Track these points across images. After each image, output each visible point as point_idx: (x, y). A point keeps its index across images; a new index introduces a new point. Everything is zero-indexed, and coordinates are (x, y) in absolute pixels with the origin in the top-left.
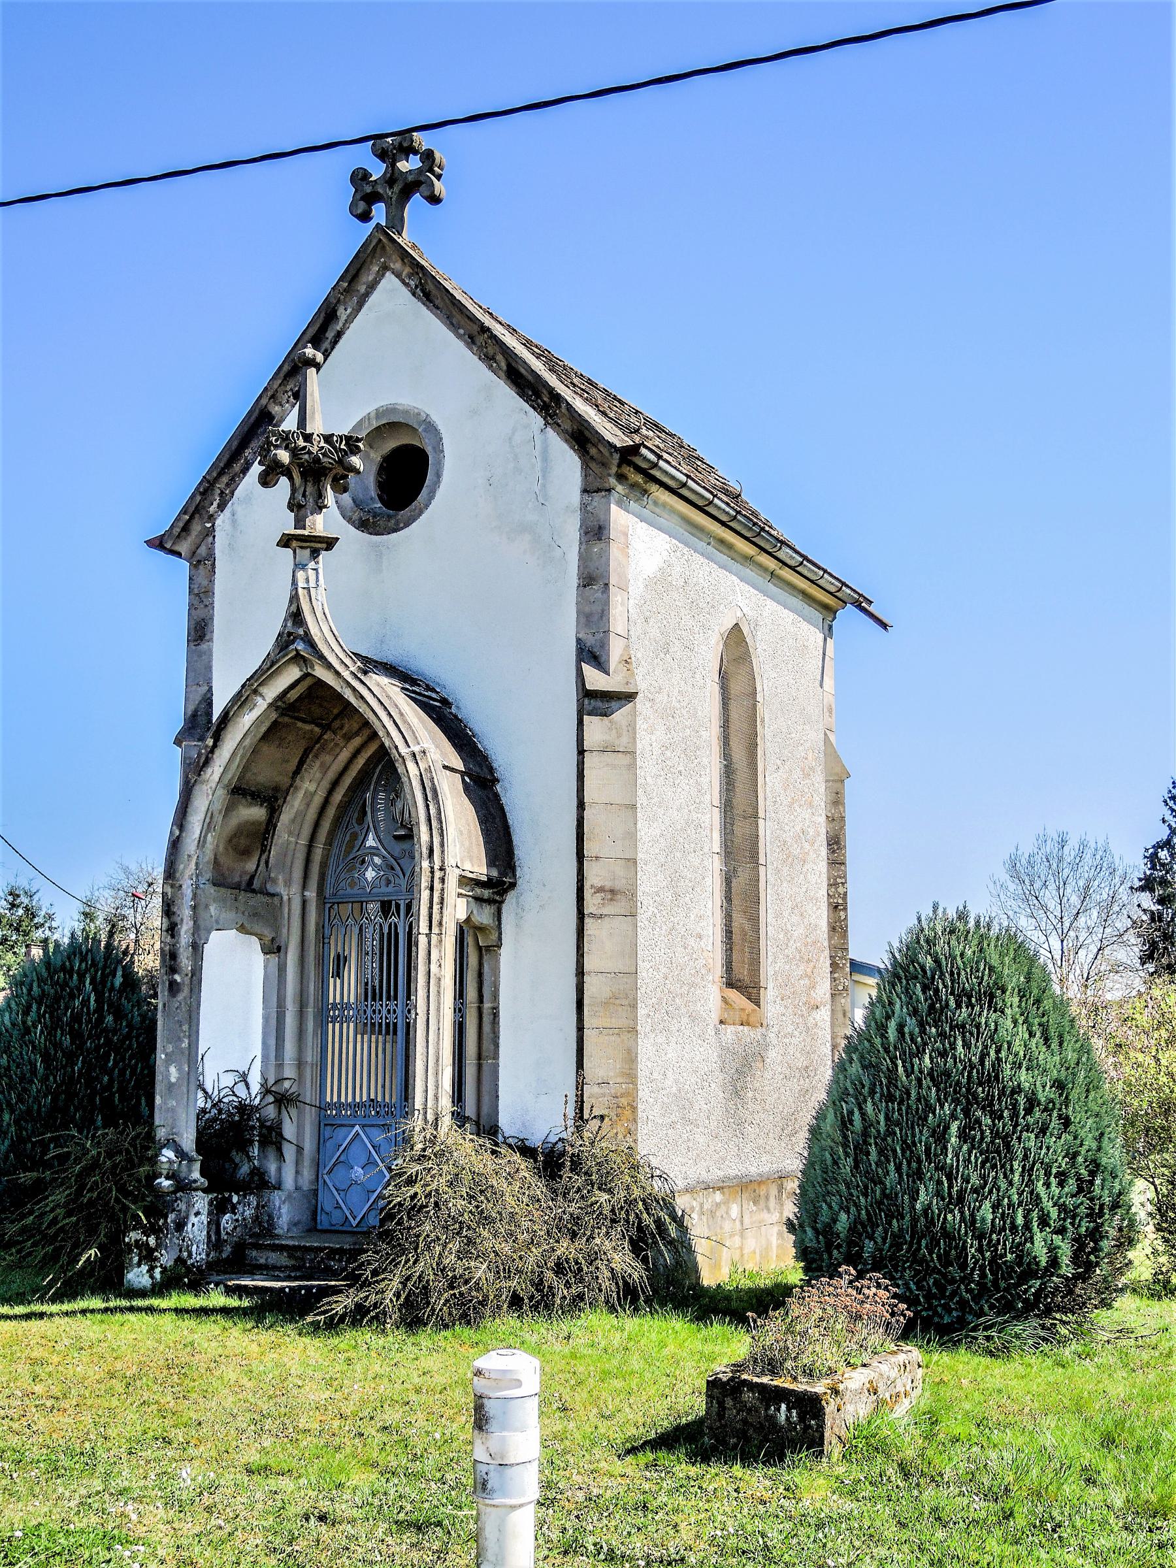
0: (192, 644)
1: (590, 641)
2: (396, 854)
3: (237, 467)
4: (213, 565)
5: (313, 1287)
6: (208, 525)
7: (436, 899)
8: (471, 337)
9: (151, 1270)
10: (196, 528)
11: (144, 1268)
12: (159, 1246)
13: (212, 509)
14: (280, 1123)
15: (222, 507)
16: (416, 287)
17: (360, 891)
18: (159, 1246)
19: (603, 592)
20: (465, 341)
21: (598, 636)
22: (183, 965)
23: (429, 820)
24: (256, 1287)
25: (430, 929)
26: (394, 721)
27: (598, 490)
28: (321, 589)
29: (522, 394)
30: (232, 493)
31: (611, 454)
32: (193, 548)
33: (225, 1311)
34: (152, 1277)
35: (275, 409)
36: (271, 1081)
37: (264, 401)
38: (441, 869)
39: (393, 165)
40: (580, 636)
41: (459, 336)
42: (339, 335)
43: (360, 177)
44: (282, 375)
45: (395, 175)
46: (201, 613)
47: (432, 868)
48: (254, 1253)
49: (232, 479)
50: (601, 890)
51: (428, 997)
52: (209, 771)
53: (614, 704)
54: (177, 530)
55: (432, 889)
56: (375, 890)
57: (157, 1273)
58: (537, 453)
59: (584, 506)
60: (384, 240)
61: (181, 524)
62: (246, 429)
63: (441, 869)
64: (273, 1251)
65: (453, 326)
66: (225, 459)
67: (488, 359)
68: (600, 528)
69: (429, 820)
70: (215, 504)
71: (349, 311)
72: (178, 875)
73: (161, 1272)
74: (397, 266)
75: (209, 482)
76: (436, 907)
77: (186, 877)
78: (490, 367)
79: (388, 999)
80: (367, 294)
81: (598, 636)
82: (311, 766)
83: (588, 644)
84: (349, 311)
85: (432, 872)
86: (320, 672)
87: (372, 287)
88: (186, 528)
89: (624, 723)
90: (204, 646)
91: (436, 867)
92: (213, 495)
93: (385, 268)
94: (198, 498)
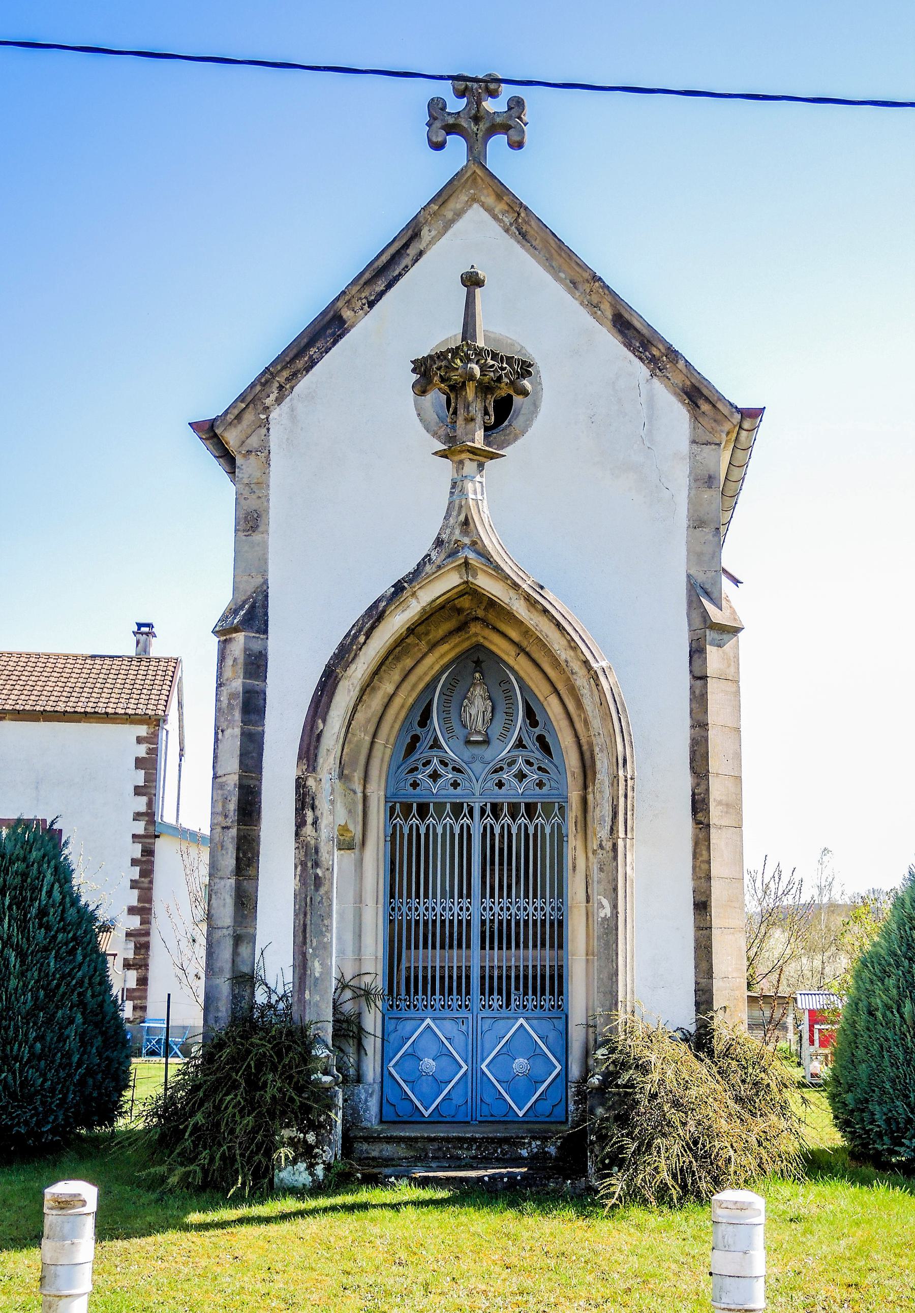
0: (241, 534)
1: (701, 578)
2: (465, 759)
3: (300, 364)
4: (268, 458)
5: (517, 1174)
6: (263, 417)
7: (629, 807)
8: (574, 283)
9: (311, 1167)
10: (249, 417)
11: (302, 1166)
12: (319, 1143)
13: (268, 402)
14: (359, 1015)
15: (279, 401)
16: (511, 224)
17: (511, 792)
18: (319, 1143)
19: (714, 536)
20: (566, 285)
21: (709, 574)
22: (323, 859)
23: (622, 732)
24: (448, 1179)
25: (626, 834)
26: (580, 636)
27: (707, 443)
28: (485, 502)
29: (628, 345)
30: (292, 388)
31: (732, 413)
32: (243, 437)
33: (419, 1204)
34: (312, 1174)
35: (347, 314)
36: (348, 977)
37: (340, 304)
38: (632, 779)
39: (479, 104)
40: (691, 572)
41: (557, 279)
42: (421, 254)
43: (436, 107)
44: (362, 281)
45: (476, 114)
46: (252, 503)
47: (626, 777)
48: (365, 1146)
49: (294, 375)
50: (720, 803)
51: (626, 897)
52: (353, 667)
53: (725, 637)
54: (230, 417)
55: (626, 796)
56: (526, 792)
57: (319, 1170)
58: (643, 399)
59: (693, 456)
60: (478, 172)
61: (236, 412)
62: (317, 328)
63: (632, 779)
64: (388, 1143)
65: (554, 271)
66: (291, 355)
67: (593, 307)
68: (710, 477)
69: (622, 732)
70: (273, 397)
71: (433, 233)
72: (318, 769)
73: (325, 1169)
74: (490, 200)
75: (272, 374)
76: (629, 813)
77: (325, 771)
78: (594, 315)
79: (461, 896)
80: (452, 221)
81: (709, 574)
82: (391, 669)
83: (699, 581)
84: (433, 233)
85: (626, 781)
86: (486, 584)
87: (459, 215)
88: (239, 417)
89: (731, 655)
90: (257, 537)
91: (629, 776)
92: (271, 387)
93: (474, 199)
94: (258, 388)
